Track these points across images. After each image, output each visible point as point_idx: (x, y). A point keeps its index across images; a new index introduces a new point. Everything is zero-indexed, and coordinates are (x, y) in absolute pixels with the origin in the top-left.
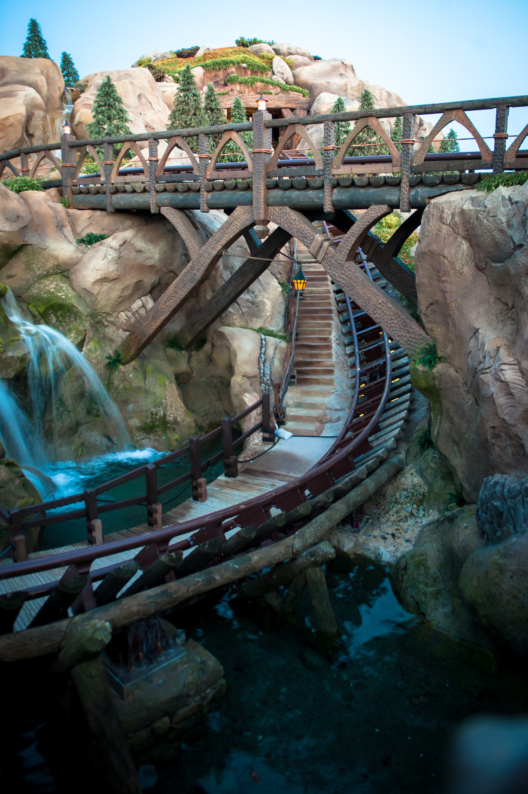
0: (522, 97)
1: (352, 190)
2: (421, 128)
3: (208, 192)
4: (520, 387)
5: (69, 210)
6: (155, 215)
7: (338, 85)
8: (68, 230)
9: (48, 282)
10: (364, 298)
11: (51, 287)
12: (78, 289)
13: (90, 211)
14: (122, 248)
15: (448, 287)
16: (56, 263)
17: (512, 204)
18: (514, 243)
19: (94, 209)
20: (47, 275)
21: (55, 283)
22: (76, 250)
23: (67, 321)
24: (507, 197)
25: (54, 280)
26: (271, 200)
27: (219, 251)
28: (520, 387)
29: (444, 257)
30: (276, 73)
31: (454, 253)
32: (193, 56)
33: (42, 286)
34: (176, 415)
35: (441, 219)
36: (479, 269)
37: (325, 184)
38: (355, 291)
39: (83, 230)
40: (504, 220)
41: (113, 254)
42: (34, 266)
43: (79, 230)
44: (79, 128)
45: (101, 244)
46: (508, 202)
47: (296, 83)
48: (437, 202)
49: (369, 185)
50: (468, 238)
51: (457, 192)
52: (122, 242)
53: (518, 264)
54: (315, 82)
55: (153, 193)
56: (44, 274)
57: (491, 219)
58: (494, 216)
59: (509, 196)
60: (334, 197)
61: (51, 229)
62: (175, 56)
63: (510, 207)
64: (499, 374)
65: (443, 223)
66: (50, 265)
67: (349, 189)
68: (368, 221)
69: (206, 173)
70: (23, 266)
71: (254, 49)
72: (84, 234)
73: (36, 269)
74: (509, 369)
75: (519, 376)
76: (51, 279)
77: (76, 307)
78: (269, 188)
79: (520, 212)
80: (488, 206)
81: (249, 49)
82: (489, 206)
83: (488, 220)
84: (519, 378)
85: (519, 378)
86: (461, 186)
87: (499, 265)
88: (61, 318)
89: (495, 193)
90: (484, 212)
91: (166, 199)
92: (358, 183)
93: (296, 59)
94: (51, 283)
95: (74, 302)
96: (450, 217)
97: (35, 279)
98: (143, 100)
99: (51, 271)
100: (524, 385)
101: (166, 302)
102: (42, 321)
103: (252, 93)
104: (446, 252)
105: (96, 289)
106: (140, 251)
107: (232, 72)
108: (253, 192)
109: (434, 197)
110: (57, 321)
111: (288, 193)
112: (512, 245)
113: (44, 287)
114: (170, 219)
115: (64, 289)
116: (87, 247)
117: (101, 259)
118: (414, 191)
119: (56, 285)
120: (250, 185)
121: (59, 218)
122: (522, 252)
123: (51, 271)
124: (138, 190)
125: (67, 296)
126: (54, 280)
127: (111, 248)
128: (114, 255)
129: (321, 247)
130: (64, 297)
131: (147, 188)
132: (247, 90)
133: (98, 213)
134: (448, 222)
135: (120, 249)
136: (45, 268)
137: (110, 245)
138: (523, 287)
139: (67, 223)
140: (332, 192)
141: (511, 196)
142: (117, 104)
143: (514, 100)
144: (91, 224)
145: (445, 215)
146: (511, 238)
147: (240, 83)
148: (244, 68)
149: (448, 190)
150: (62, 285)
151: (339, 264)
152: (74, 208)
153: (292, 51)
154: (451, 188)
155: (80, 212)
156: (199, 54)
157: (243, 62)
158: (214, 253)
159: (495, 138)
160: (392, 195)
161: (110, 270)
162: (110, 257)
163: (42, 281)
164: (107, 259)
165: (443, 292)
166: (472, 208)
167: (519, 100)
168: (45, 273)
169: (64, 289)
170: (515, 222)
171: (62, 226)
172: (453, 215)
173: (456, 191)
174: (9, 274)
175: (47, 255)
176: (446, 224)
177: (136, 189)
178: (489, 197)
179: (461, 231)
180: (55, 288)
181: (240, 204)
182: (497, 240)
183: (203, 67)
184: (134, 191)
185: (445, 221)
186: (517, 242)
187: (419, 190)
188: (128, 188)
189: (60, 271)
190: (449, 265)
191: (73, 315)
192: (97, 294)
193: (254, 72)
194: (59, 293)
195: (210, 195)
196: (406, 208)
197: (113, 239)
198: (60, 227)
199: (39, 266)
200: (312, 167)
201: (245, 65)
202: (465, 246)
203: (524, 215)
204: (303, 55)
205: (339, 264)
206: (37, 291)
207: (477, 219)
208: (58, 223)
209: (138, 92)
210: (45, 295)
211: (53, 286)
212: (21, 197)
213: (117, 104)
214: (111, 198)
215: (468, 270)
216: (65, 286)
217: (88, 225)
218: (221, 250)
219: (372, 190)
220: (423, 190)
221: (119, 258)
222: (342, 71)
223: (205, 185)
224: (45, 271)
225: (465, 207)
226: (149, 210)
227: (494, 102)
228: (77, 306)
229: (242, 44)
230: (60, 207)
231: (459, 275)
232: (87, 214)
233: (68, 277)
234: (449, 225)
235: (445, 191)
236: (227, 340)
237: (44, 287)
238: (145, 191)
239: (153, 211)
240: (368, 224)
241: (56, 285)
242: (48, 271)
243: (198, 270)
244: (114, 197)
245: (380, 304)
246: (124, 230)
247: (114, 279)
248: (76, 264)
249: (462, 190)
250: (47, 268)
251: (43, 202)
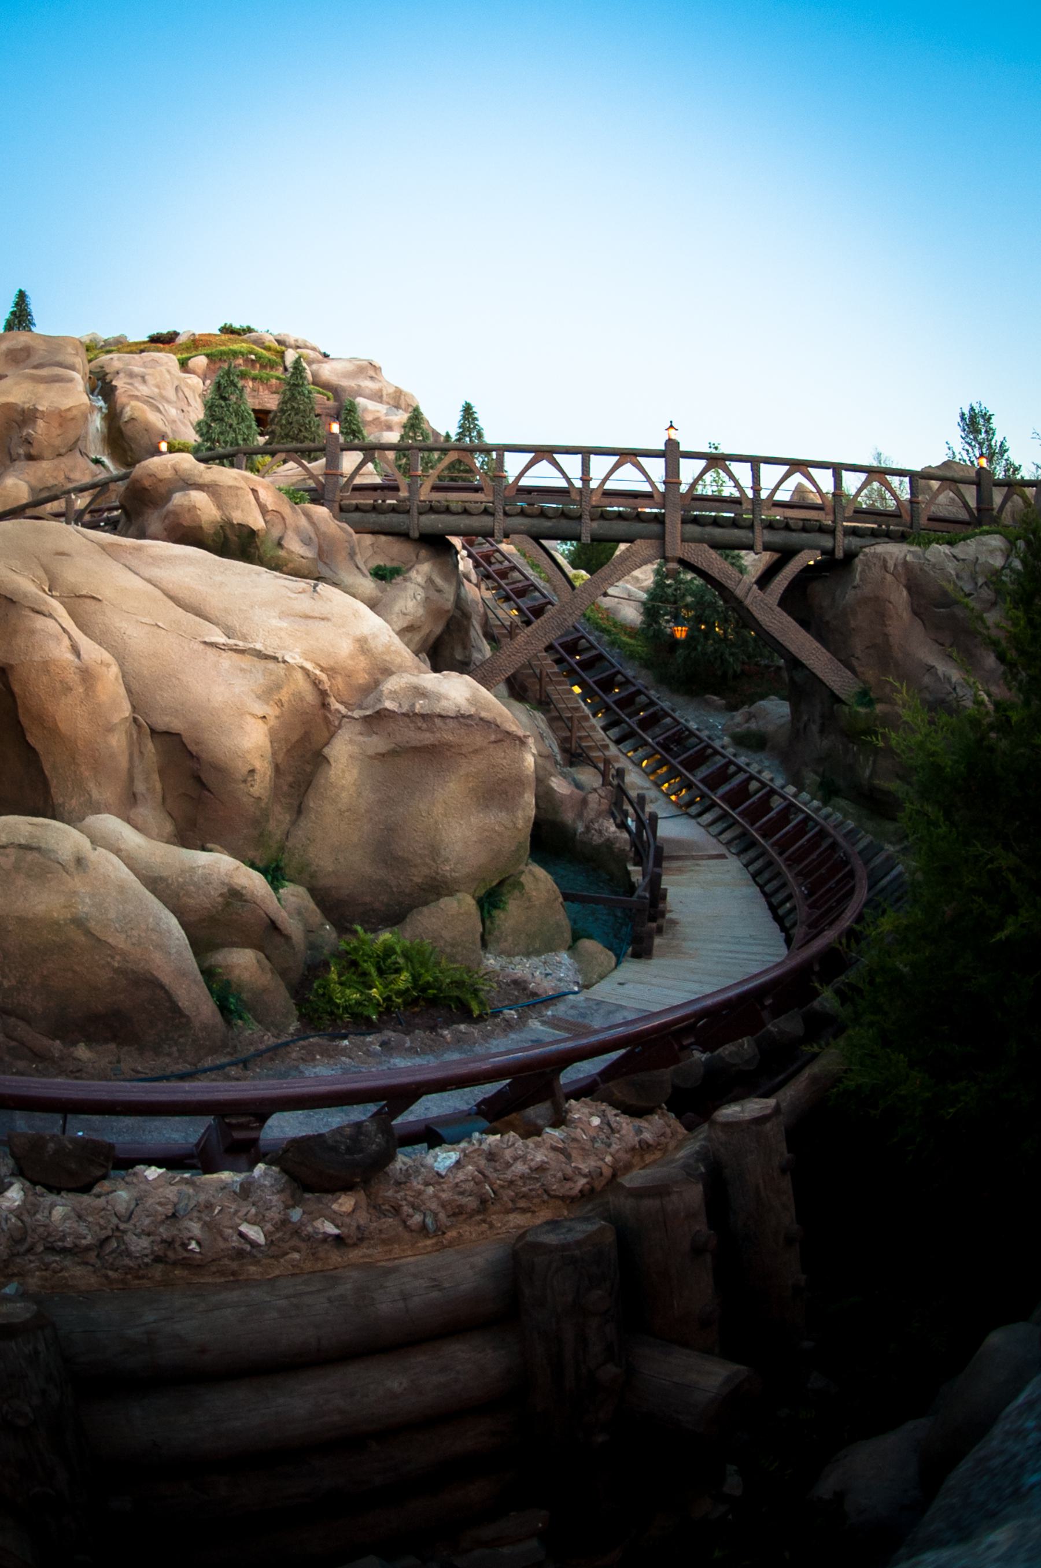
3: (592, 520)
7: (371, 390)
15: (890, 630)
26: (687, 536)
29: (890, 602)
32: (174, 342)
35: (885, 567)
36: (915, 613)
37: (755, 523)
40: (953, 572)
44: (129, 426)
45: (405, 580)
49: (804, 530)
50: (909, 588)
54: (342, 384)
55: (500, 515)
61: (342, 556)
67: (780, 532)
69: (590, 498)
71: (252, 338)
78: (684, 522)
81: (245, 337)
82: (933, 560)
83: (935, 572)
86: (887, 540)
87: (942, 610)
91: (521, 524)
92: (793, 527)
93: (308, 354)
98: (180, 394)
103: (266, 392)
104: (892, 598)
107: (240, 365)
109: (865, 547)
132: (261, 387)
133: (383, 538)
145: (889, 565)
147: (254, 379)
148: (252, 360)
153: (300, 344)
154: (878, 540)
156: (180, 340)
157: (251, 353)
160: (827, 542)
165: (885, 634)
170: (965, 575)
172: (895, 566)
179: (903, 580)
181: (641, 538)
183: (207, 356)
188: (453, 506)
193: (263, 367)
195: (595, 525)
200: (738, 506)
201: (253, 357)
202: (905, 593)
204: (314, 349)
207: (921, 570)
209: (176, 383)
214: (418, 519)
215: (906, 615)
219: (804, 535)
222: (372, 373)
223: (590, 512)
229: (227, 330)
234: (893, 574)
243: (570, 614)
244: (424, 519)
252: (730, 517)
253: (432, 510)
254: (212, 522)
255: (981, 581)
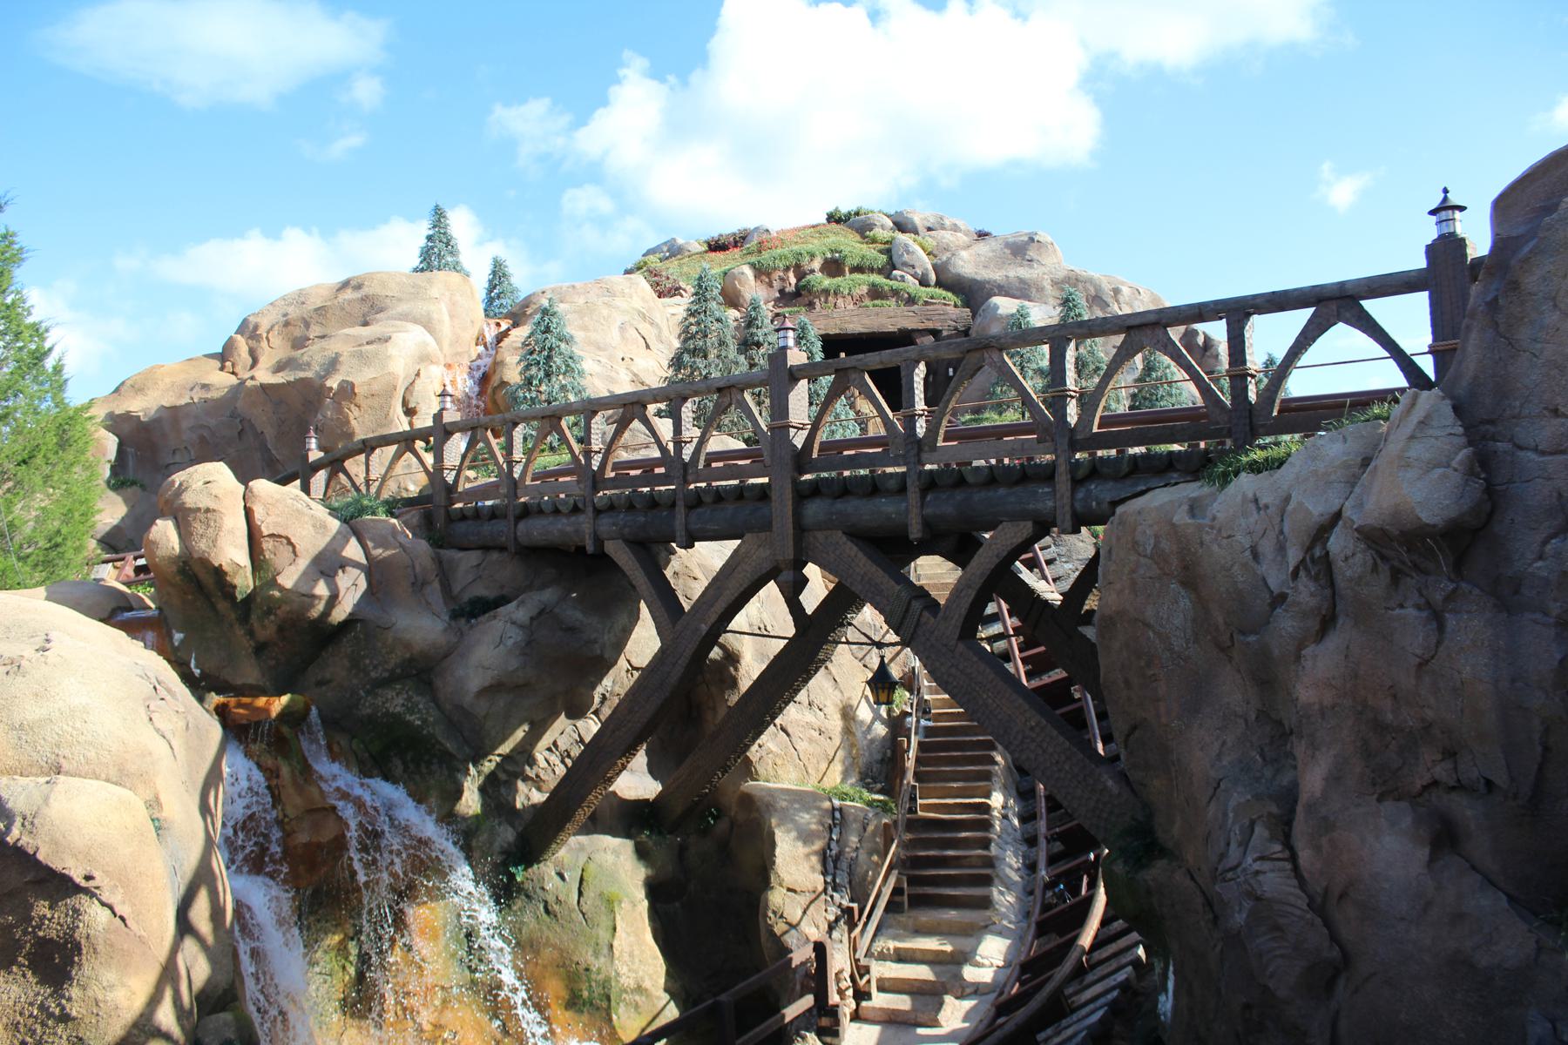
0: (1285, 292)
1: (959, 495)
2: (1208, 354)
4: (1298, 912)
5: (442, 552)
6: (593, 556)
8: (434, 590)
9: (390, 694)
10: (999, 717)
11: (395, 702)
12: (448, 707)
13: (478, 553)
14: (535, 623)
16: (408, 655)
17: (1259, 509)
18: (1272, 592)
19: (486, 548)
20: (386, 683)
21: (405, 696)
22: (445, 630)
23: (424, 770)
24: (1250, 495)
25: (403, 689)
27: (713, 625)
28: (1298, 912)
29: (1148, 625)
30: (897, 266)
31: (1165, 616)
33: (379, 701)
34: (641, 973)
38: (981, 702)
39: (462, 590)
41: (515, 636)
42: (367, 661)
43: (456, 588)
45: (495, 617)
46: (1252, 506)
47: (939, 284)
48: (1125, 512)
51: (1165, 489)
52: (534, 612)
53: (1282, 636)
56: (384, 678)
57: (1225, 541)
58: (1229, 537)
59: (1255, 495)
60: (928, 511)
62: (705, 248)
63: (1256, 516)
64: (1252, 881)
65: (1139, 554)
66: (394, 660)
68: (997, 556)
70: (346, 663)
72: (466, 597)
73: (371, 668)
74: (1273, 871)
75: (1295, 887)
76: (398, 687)
77: (442, 744)
79: (1273, 526)
80: (1218, 515)
83: (1219, 546)
84: (1292, 890)
85: (1292, 890)
88: (412, 766)
89: (1232, 488)
90: (1212, 527)
94: (397, 695)
95: (439, 732)
96: (1152, 541)
97: (368, 687)
99: (398, 671)
100: (1305, 907)
101: (614, 732)
102: (375, 772)
105: (482, 708)
106: (571, 630)
108: (773, 504)
109: (1123, 501)
110: (405, 771)
111: (840, 505)
112: (1268, 596)
113: (384, 703)
114: (620, 564)
115: (421, 706)
116: (468, 621)
117: (492, 647)
118: (1083, 489)
119: (405, 700)
120: (768, 492)
121: (418, 569)
122: (1286, 611)
123: (398, 671)
124: (563, 509)
125: (424, 721)
126: (403, 689)
127: (513, 623)
128: (519, 638)
129: (907, 610)
130: (419, 723)
131: (580, 505)
133: (495, 555)
134: (1149, 552)
135: (531, 624)
136: (386, 666)
137: (511, 619)
138: (1294, 687)
139: (433, 577)
140: (923, 497)
141: (1258, 495)
142: (563, 346)
143: (1258, 301)
144: (480, 577)
146: (1264, 579)
149: (1148, 485)
150: (419, 698)
151: (946, 645)
152: (453, 547)
154: (1153, 482)
155: (461, 554)
156: (752, 244)
158: (704, 628)
159: (1230, 377)
161: (511, 669)
162: (510, 642)
163: (380, 691)
164: (505, 645)
166: (1190, 521)
167: (1268, 301)
168: (386, 675)
169: (421, 706)
171: (424, 583)
172: (1157, 537)
173: (1165, 486)
174: (319, 678)
175: (390, 640)
176: (1145, 556)
177: (561, 508)
178: (1221, 497)
180: (403, 705)
182: (1240, 586)
184: (557, 511)
185: (1141, 548)
186: (1276, 592)
187: (1093, 487)
189: (414, 672)
190: (1157, 642)
191: (435, 761)
192: (485, 717)
194: (411, 715)
196: (1068, 524)
197: (518, 606)
198: (419, 585)
199: (375, 662)
203: (1281, 532)
205: (946, 645)
206: (369, 711)
208: (415, 576)
210: (385, 720)
211: (400, 701)
212: (352, 529)
213: (563, 346)
216: (422, 702)
217: (474, 581)
218: (716, 622)
220: (1099, 489)
221: (529, 643)
224: (386, 670)
225: (1176, 519)
226: (584, 548)
227: (1220, 307)
228: (443, 741)
230: (423, 546)
231: (1182, 663)
232: (473, 557)
233: (430, 684)
234: (1151, 558)
235: (1144, 488)
236: (758, 810)
237: (384, 703)
238: (576, 510)
239: (590, 549)
240: (998, 561)
241: (405, 700)
242: (392, 671)
245: (1032, 729)
246: (543, 587)
247: (518, 687)
248: (446, 656)
249: (1176, 484)
250: (390, 666)
251: (391, 539)
252: (762, 484)
253: (526, 512)
254: (170, 558)
255: (1294, 556)
